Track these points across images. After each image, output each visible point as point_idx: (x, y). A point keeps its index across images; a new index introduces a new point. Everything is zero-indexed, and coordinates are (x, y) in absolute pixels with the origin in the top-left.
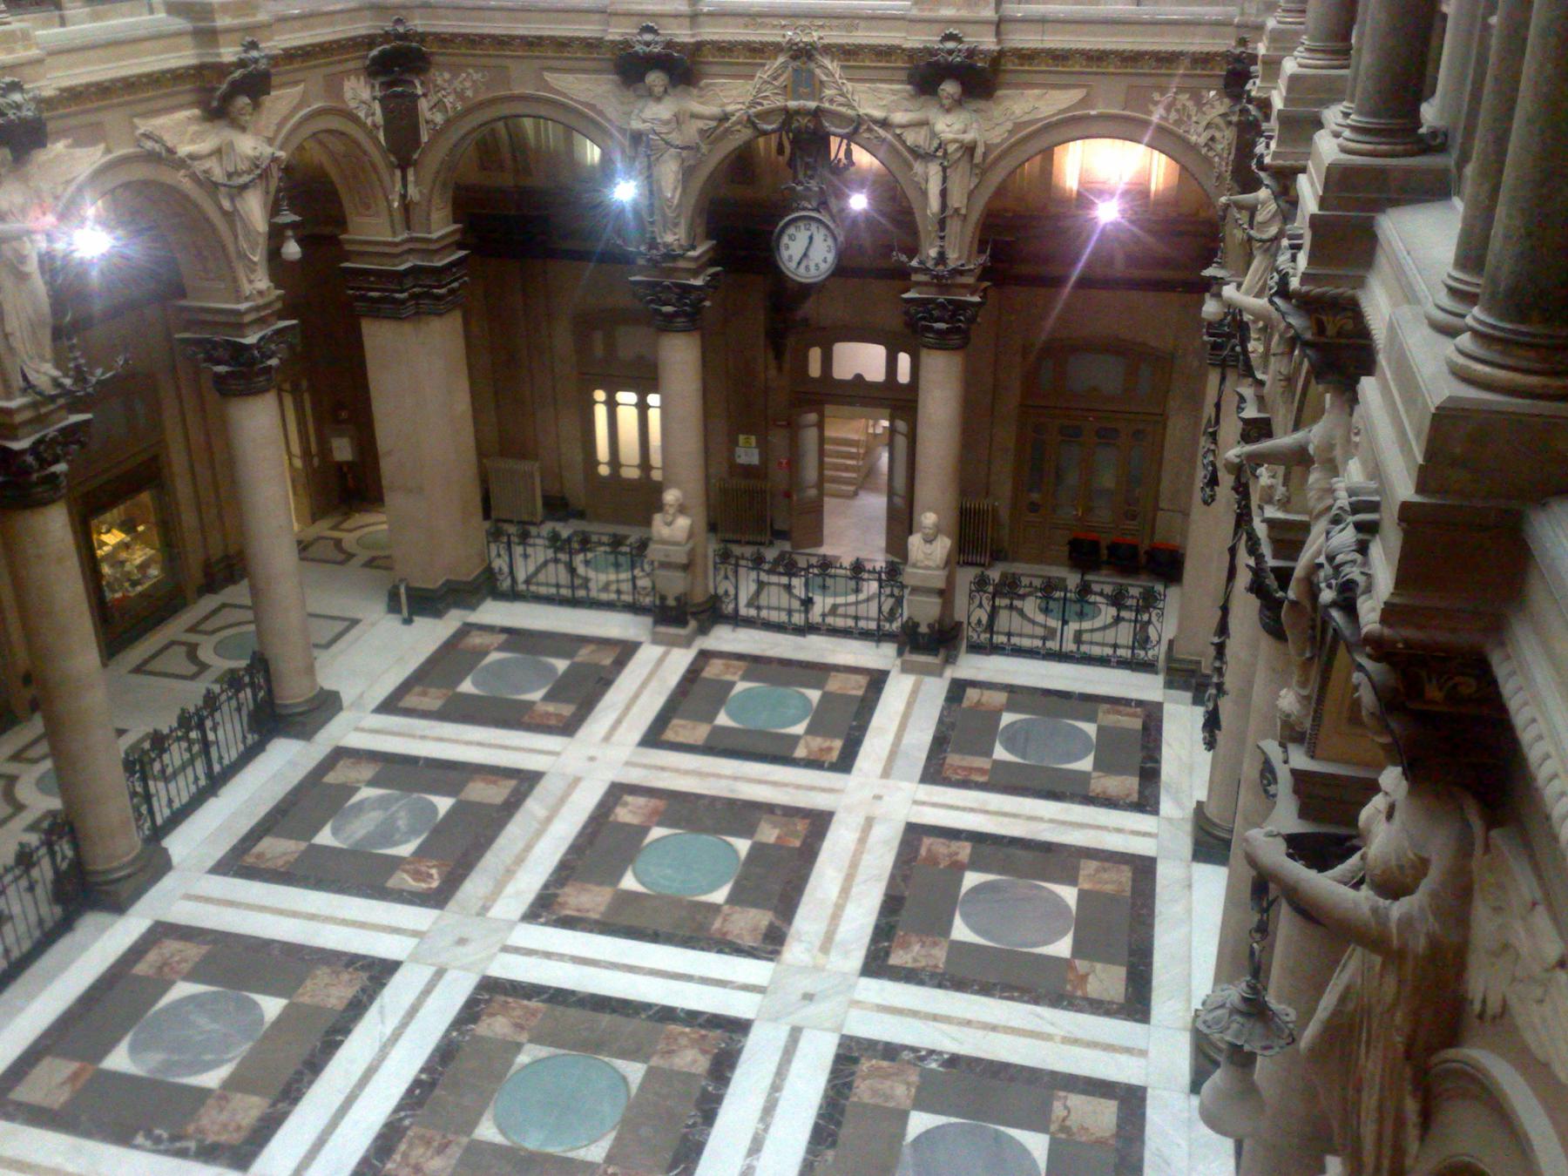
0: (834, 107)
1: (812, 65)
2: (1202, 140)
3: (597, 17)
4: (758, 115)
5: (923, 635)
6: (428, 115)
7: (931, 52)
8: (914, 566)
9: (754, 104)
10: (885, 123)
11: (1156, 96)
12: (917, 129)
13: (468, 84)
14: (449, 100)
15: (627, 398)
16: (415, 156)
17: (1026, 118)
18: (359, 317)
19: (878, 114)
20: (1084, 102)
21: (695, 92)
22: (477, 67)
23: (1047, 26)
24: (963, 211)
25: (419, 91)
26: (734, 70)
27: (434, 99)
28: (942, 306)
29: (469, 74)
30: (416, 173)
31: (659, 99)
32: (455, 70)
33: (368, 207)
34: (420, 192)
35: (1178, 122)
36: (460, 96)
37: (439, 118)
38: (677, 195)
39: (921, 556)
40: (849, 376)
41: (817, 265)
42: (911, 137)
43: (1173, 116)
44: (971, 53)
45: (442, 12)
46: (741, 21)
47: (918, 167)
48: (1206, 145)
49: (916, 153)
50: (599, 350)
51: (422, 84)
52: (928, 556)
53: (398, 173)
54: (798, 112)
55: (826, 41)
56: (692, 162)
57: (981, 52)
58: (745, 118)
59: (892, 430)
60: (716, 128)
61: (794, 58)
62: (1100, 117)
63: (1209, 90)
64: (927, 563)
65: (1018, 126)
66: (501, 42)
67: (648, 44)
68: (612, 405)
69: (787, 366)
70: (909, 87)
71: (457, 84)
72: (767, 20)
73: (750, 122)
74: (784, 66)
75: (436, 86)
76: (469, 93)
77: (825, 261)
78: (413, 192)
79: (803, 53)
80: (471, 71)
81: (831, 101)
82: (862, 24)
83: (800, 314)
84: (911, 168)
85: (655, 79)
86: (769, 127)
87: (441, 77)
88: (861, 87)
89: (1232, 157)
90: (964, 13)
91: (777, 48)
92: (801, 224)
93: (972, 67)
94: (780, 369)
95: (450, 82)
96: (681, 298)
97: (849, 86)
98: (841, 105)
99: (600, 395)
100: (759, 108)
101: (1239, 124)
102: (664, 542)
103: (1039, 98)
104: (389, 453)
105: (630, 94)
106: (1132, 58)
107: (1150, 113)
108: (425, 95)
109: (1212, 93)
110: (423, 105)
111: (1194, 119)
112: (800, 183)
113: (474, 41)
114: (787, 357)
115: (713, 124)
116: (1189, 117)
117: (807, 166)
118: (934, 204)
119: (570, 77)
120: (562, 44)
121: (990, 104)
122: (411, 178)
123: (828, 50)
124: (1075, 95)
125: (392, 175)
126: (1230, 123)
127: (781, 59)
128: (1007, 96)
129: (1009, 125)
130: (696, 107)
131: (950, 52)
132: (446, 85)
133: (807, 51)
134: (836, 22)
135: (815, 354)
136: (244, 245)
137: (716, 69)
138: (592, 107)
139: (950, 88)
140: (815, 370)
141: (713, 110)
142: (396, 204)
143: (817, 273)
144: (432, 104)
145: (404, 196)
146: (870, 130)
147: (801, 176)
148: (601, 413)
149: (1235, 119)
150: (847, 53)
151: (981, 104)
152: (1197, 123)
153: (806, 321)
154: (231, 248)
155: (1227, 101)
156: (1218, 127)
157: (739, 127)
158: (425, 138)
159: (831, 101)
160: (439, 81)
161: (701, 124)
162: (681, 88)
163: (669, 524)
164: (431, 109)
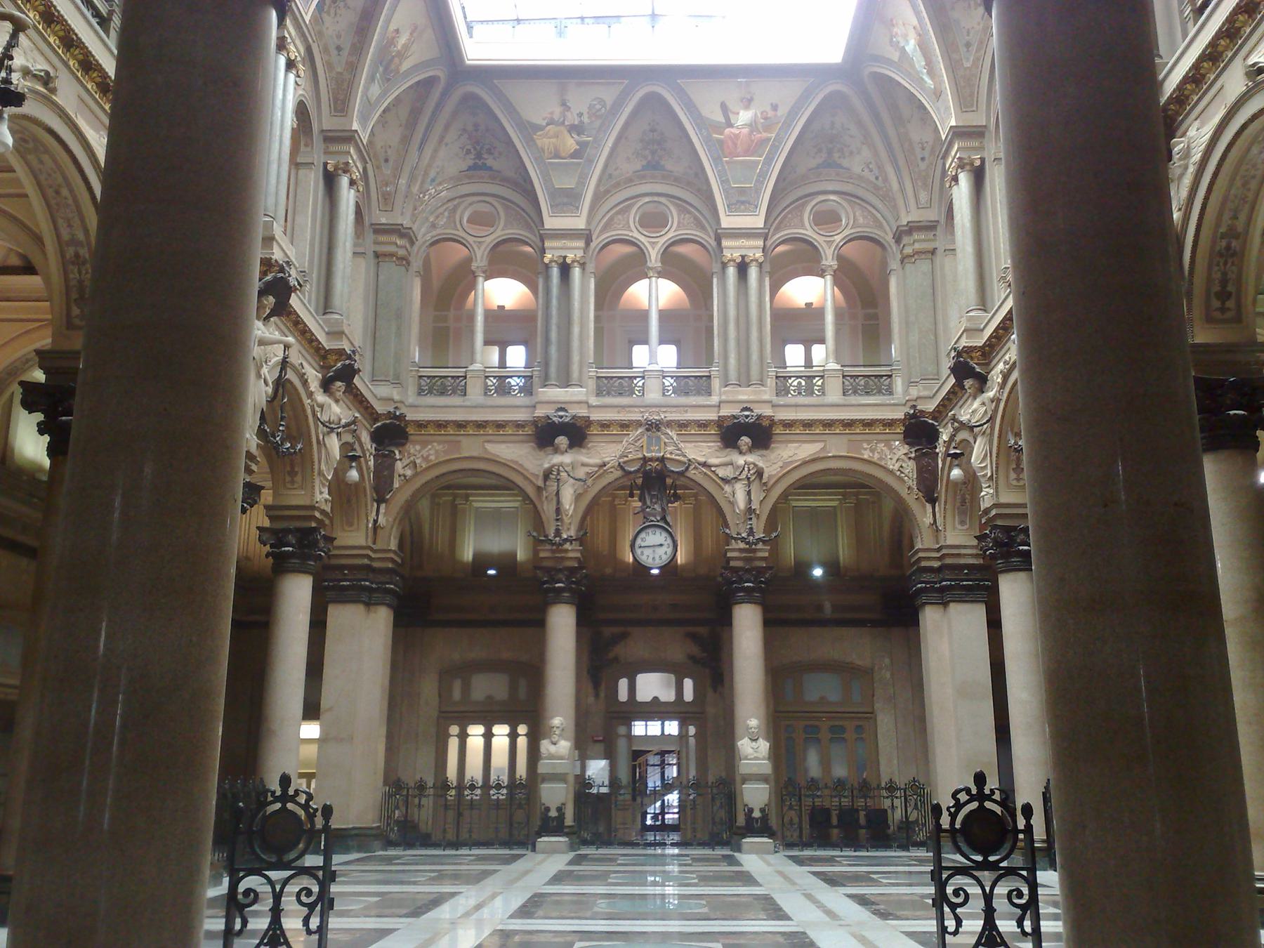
0: (673, 457)
1: (659, 433)
2: (897, 467)
3: (523, 410)
4: (624, 462)
5: (757, 820)
6: (402, 472)
7: (734, 417)
8: (746, 758)
9: (621, 457)
10: (704, 464)
11: (865, 446)
12: (725, 467)
13: (432, 452)
14: (418, 461)
15: (476, 731)
16: (388, 497)
17: (790, 460)
18: (328, 603)
19: (702, 459)
20: (823, 449)
21: (584, 451)
22: (439, 443)
23: (798, 408)
24: (758, 512)
25: (398, 457)
26: (609, 438)
27: (406, 461)
28: (747, 571)
29: (433, 446)
30: (387, 508)
31: (562, 453)
32: (424, 444)
33: (351, 524)
34: (387, 520)
35: (881, 459)
36: (426, 459)
37: (409, 473)
38: (573, 507)
39: (750, 751)
40: (649, 699)
41: (660, 557)
42: (721, 472)
43: (876, 456)
44: (759, 417)
45: (421, 409)
46: (616, 410)
47: (727, 488)
48: (899, 470)
49: (724, 480)
50: (457, 694)
51: (400, 452)
52: (756, 750)
53: (375, 505)
54: (651, 459)
55: (668, 419)
56: (580, 491)
57: (764, 417)
58: (617, 464)
59: (683, 736)
60: (596, 472)
61: (648, 430)
62: (833, 457)
63: (895, 441)
64: (755, 755)
65: (786, 464)
66: (460, 425)
67: (561, 417)
68: (463, 737)
69: (602, 695)
70: (719, 444)
71: (424, 453)
72: (632, 409)
73: (621, 466)
74: (642, 434)
75: (409, 454)
76: (432, 458)
77: (666, 553)
78: (381, 520)
79: (653, 427)
80: (435, 444)
81: (671, 453)
82: (689, 409)
83: (611, 655)
84: (723, 489)
85: (562, 441)
86: (632, 469)
87: (412, 448)
88: (688, 445)
89: (915, 477)
90: (752, 398)
91: (638, 424)
92: (650, 531)
93: (760, 425)
94: (597, 696)
95: (420, 451)
96: (568, 578)
97: (682, 445)
98: (676, 455)
99: (454, 730)
100: (626, 459)
101: (916, 457)
102: (552, 757)
103: (797, 448)
104: (330, 709)
105: (542, 453)
106: (849, 424)
107: (863, 455)
108: (401, 460)
109: (897, 443)
110: (399, 465)
111: (889, 457)
113: (440, 425)
114: (603, 687)
115: (597, 469)
116: (886, 456)
117: (652, 497)
119: (503, 446)
120: (500, 425)
121: (768, 452)
122: (382, 510)
123: (669, 424)
124: (820, 445)
125: (372, 506)
126: (910, 458)
127: (640, 430)
128: (777, 447)
129: (780, 464)
130: (585, 460)
131: (747, 417)
132: (416, 453)
133: (657, 425)
134: (674, 409)
135: (623, 684)
136: (323, 467)
137: (599, 439)
138: (516, 462)
139: (745, 440)
140: (623, 695)
141: (597, 461)
142: (370, 525)
143: (660, 562)
144: (405, 464)
145: (375, 521)
146: (696, 468)
147: (648, 503)
148: (453, 744)
149: (913, 455)
150: (682, 425)
151: (764, 452)
152: (891, 459)
153: (616, 659)
154: (316, 467)
155: (906, 446)
156: (903, 461)
157: (612, 470)
158: (396, 485)
159: (671, 453)
160: (412, 451)
161: (588, 469)
162: (575, 449)
164: (404, 468)
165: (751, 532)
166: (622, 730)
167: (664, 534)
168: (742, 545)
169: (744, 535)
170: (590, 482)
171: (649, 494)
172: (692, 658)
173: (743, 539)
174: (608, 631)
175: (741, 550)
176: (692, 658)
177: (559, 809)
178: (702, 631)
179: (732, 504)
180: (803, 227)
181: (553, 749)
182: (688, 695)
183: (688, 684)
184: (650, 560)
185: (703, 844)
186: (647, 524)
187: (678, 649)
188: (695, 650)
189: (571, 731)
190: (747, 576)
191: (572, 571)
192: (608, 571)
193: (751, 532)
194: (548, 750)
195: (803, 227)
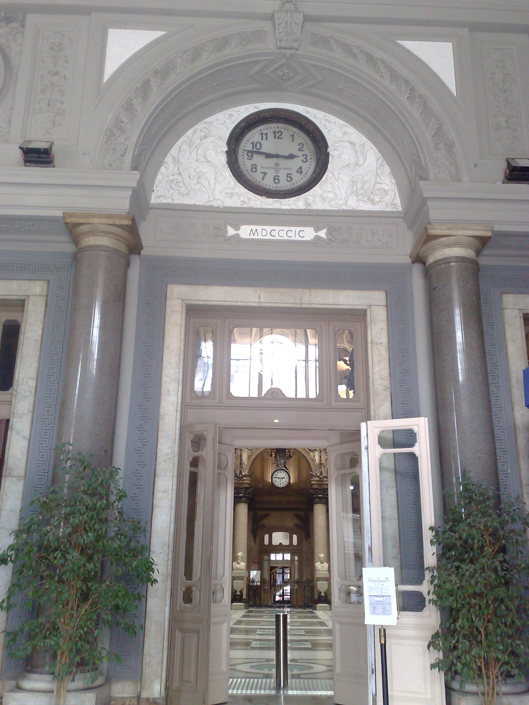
28: (320, 490)
38: (247, 461)
47: (311, 454)
59: (292, 560)
69: (257, 541)
83: (261, 524)
84: (310, 454)
92: (279, 471)
112: (279, 461)
117: (280, 457)
118: (317, 461)
135: (267, 537)
140: (266, 542)
147: (278, 459)
153: (263, 526)
163: (239, 564)
165: (321, 473)
166: (266, 558)
167: (285, 473)
168: (318, 479)
169: (318, 475)
170: (254, 451)
171: (279, 455)
172: (296, 525)
173: (318, 476)
174: (260, 513)
175: (317, 481)
176: (296, 525)
177: (241, 591)
178: (301, 513)
179: (314, 460)
180: (344, 343)
181: (238, 566)
182: (295, 542)
183: (295, 537)
184: (279, 484)
185: (300, 607)
186: (278, 468)
187: (290, 521)
188: (297, 521)
189: (245, 557)
190: (319, 492)
191: (246, 488)
192: (260, 486)
193: (321, 473)
194: (236, 566)
195: (344, 343)
